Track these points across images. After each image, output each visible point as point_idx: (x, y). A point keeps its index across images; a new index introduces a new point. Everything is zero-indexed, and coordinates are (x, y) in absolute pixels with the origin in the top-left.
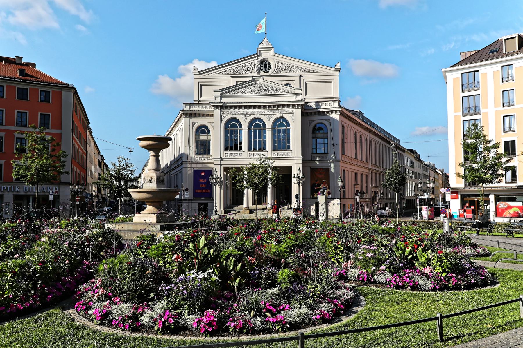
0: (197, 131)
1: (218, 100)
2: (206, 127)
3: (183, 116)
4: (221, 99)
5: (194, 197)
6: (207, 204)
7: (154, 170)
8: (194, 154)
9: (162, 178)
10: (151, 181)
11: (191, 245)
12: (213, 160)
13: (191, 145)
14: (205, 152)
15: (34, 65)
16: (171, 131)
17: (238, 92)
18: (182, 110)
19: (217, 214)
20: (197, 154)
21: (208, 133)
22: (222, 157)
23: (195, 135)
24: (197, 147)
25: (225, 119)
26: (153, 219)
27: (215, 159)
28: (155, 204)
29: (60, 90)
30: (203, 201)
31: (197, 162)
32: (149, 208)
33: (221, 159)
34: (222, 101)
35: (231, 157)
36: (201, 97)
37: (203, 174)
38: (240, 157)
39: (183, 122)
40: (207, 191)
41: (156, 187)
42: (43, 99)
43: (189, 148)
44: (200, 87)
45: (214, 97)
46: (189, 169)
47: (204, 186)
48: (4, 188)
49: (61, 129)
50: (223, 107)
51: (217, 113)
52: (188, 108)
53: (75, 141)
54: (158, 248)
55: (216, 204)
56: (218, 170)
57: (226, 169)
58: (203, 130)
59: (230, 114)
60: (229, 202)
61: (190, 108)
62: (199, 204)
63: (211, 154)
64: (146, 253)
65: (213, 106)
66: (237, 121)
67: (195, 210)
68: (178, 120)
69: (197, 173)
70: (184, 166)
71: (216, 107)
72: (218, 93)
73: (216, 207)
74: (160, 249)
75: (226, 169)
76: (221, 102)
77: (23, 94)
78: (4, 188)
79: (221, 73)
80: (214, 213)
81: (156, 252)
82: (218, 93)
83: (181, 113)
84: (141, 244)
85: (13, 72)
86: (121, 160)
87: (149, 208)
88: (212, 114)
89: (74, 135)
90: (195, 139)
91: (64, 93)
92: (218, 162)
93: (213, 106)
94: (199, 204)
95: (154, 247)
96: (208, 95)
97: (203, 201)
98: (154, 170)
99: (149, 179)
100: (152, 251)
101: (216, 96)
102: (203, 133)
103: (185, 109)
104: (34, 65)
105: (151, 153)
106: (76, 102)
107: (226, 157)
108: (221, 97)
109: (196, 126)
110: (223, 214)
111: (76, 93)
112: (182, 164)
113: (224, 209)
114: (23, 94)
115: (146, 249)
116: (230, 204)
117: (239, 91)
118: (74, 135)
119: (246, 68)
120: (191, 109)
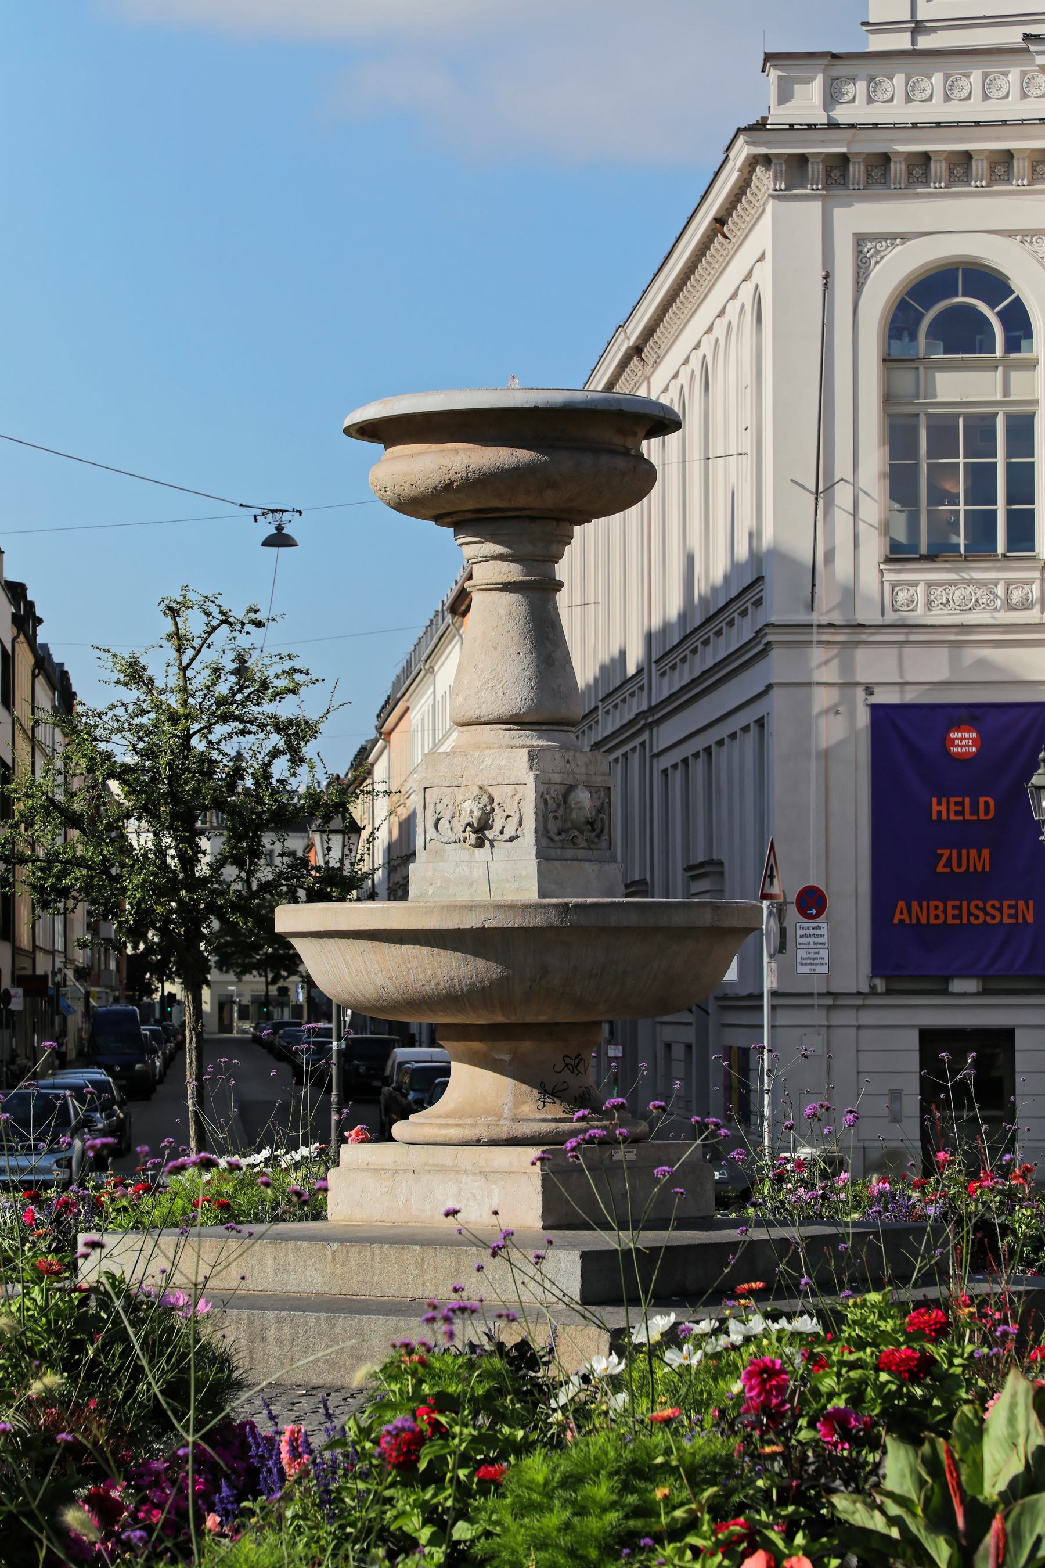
0: (901, 321)
3: (764, 180)
5: (878, 967)
6: (1006, 1037)
7: (514, 721)
8: (873, 548)
9: (583, 798)
10: (481, 830)
11: (897, 1466)
16: (649, 332)
18: (761, 125)
20: (898, 554)
21: (1013, 345)
23: (888, 360)
24: (901, 484)
26: (510, 1192)
28: (526, 1046)
30: (966, 1008)
31: (905, 632)
32: (475, 1089)
37: (964, 742)
41: (530, 894)
43: (823, 492)
46: (823, 698)
47: (979, 859)
52: (808, 102)
54: (572, 1481)
64: (462, 1531)
67: (895, 1095)
68: (720, 221)
69: (903, 736)
70: (779, 666)
74: (602, 1490)
81: (554, 1520)
83: (742, 151)
84: (418, 1440)
86: (194, 623)
87: (475, 1089)
90: (888, 399)
95: (537, 1467)
97: (966, 1008)
98: (514, 721)
99: (470, 810)
100: (523, 1509)
102: (964, 336)
103: (780, 115)
105: (484, 561)
109: (894, 271)
112: (756, 650)
115: (463, 1491)
120: (842, 114)
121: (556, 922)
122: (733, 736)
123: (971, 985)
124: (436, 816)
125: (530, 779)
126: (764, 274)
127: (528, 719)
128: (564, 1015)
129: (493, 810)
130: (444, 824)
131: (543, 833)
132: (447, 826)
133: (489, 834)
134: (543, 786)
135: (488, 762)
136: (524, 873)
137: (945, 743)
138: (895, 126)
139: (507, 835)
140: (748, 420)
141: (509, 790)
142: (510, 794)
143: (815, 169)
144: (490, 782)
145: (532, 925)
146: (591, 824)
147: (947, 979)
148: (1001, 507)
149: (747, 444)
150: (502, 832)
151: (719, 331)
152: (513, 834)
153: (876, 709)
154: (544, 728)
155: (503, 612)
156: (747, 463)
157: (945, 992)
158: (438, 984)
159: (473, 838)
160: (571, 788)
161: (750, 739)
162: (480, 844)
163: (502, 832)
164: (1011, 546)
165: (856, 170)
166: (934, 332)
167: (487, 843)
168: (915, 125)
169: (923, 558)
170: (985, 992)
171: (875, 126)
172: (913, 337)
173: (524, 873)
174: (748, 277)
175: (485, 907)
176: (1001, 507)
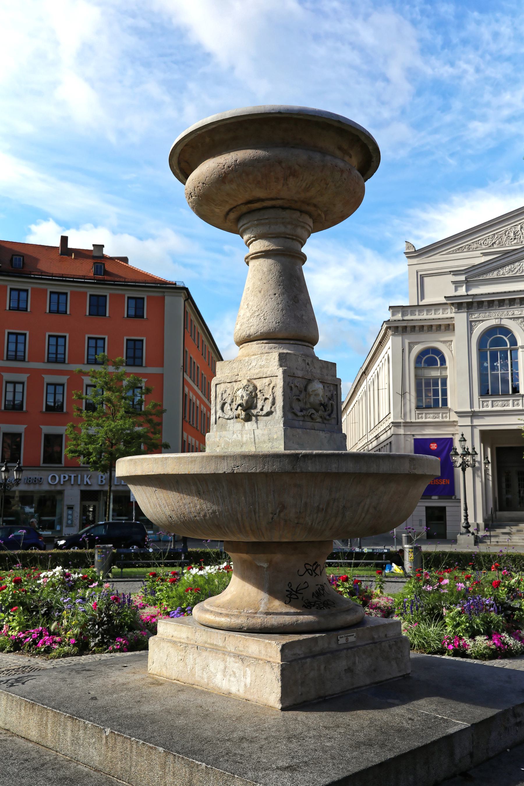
1: (462, 291)
2: (437, 352)
3: (390, 332)
4: (467, 290)
6: (443, 509)
9: (317, 387)
12: (454, 417)
13: (408, 390)
14: (436, 401)
15: (125, 260)
16: (366, 368)
17: (505, 272)
19: (469, 532)
20: (418, 408)
21: (441, 364)
22: (476, 409)
23: (416, 368)
25: (479, 329)
27: (461, 414)
28: (278, 557)
29: (160, 295)
30: (435, 502)
33: (474, 415)
34: (470, 293)
35: (495, 409)
36: (423, 298)
37: (434, 446)
38: (516, 408)
39: (389, 344)
40: (443, 482)
42: (132, 312)
44: (421, 279)
45: (453, 286)
48: (65, 477)
49: (162, 366)
50: (471, 305)
51: (460, 320)
52: (399, 316)
53: (191, 389)
55: (466, 509)
56: (468, 437)
57: (487, 436)
58: (432, 358)
59: (489, 320)
60: (491, 505)
61: (403, 315)
62: (427, 508)
63: (449, 405)
65: (452, 304)
66: (507, 331)
67: (421, 521)
68: (380, 342)
71: (459, 306)
72: (462, 278)
73: (466, 516)
75: (487, 436)
76: (468, 295)
77: (98, 306)
78: (65, 477)
79: (461, 250)
80: (463, 530)
82: (462, 278)
83: (385, 326)
85: (86, 269)
88: (449, 325)
89: (187, 378)
90: (416, 376)
91: (168, 299)
92: (467, 421)
93: (452, 304)
94: (427, 508)
96: (440, 290)
97: (435, 502)
101: (457, 284)
102: (431, 363)
104: (125, 260)
106: (193, 318)
107: (485, 409)
108: (468, 283)
109: (417, 349)
110: (481, 534)
111: (189, 298)
113: (485, 520)
114: (98, 306)
116: (495, 510)
117: (507, 268)
118: (187, 378)
119: (512, 235)
120: (406, 318)
121: (288, 467)
122: (385, 446)
123: (436, 497)
124: (222, 402)
125: (280, 372)
126: (390, 352)
127: (280, 336)
128: (300, 537)
129: (256, 395)
130: (227, 407)
131: (287, 409)
132: (229, 408)
133: (254, 412)
134: (289, 377)
135: (253, 364)
136: (275, 437)
137: (429, 447)
138: (416, 320)
139: (264, 412)
140: (387, 381)
141: (267, 381)
142: (267, 384)
143: (400, 329)
144: (255, 377)
145: (270, 471)
146: (324, 406)
147: (431, 496)
148: (440, 397)
149: (387, 386)
150: (262, 410)
151: (381, 365)
152: (269, 410)
153: (415, 440)
154: (292, 342)
155: (265, 269)
156: (387, 390)
157: (431, 499)
158: (205, 516)
159: (243, 414)
160: (309, 381)
161: (388, 446)
162: (248, 419)
163: (262, 410)
164: (443, 405)
165: (408, 329)
166: (425, 362)
167: (254, 418)
168: (420, 320)
169: (424, 408)
170: (439, 499)
171: (412, 320)
172: (421, 363)
173: (275, 437)
174: (386, 353)
175: (234, 457)
176: (440, 397)
